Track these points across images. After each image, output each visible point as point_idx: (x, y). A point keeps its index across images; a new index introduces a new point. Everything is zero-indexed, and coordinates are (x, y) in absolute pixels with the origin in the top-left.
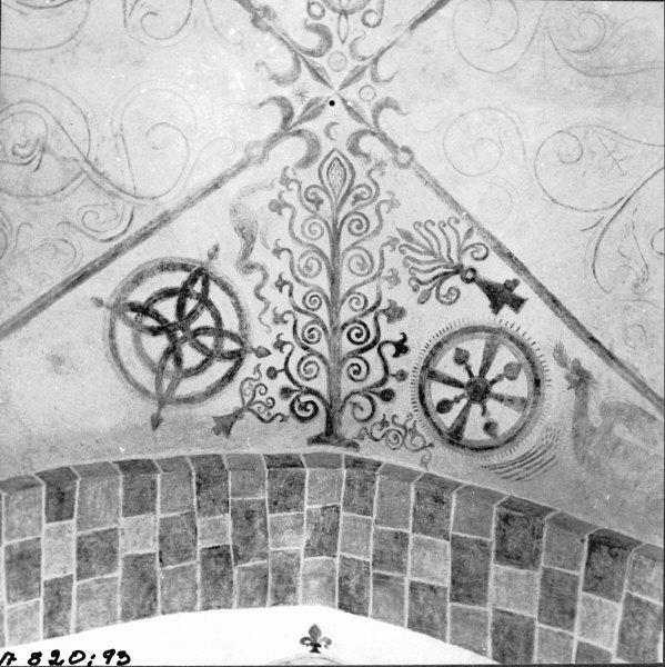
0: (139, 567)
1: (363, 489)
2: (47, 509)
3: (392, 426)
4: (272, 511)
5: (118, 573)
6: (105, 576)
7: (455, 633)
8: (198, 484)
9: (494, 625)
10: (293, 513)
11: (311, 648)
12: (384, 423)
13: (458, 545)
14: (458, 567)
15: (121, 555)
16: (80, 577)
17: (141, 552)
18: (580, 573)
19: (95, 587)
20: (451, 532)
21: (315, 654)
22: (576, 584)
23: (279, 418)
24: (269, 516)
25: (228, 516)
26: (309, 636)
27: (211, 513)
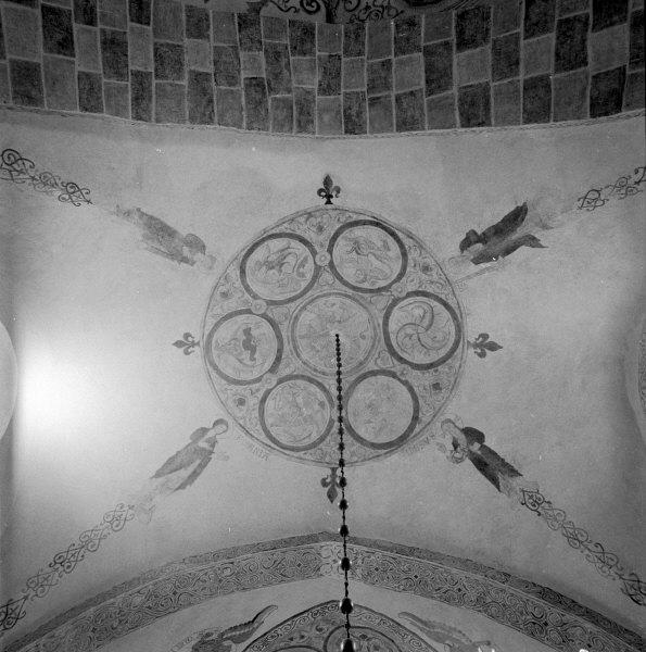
0: (199, 78)
1: (357, 36)
2: (130, 10)
3: (373, 8)
4: (293, 55)
5: (185, 83)
6: (176, 82)
7: (432, 120)
8: (240, 25)
9: (460, 99)
10: (308, 57)
11: (325, 200)
12: (367, 7)
13: (428, 52)
14: (429, 69)
15: (186, 69)
16: (157, 76)
17: (201, 70)
18: (521, 30)
19: (169, 88)
20: (423, 44)
21: (329, 206)
22: (518, 38)
23: (293, 10)
24: (291, 58)
25: (262, 53)
26: (323, 187)
27: (250, 50)
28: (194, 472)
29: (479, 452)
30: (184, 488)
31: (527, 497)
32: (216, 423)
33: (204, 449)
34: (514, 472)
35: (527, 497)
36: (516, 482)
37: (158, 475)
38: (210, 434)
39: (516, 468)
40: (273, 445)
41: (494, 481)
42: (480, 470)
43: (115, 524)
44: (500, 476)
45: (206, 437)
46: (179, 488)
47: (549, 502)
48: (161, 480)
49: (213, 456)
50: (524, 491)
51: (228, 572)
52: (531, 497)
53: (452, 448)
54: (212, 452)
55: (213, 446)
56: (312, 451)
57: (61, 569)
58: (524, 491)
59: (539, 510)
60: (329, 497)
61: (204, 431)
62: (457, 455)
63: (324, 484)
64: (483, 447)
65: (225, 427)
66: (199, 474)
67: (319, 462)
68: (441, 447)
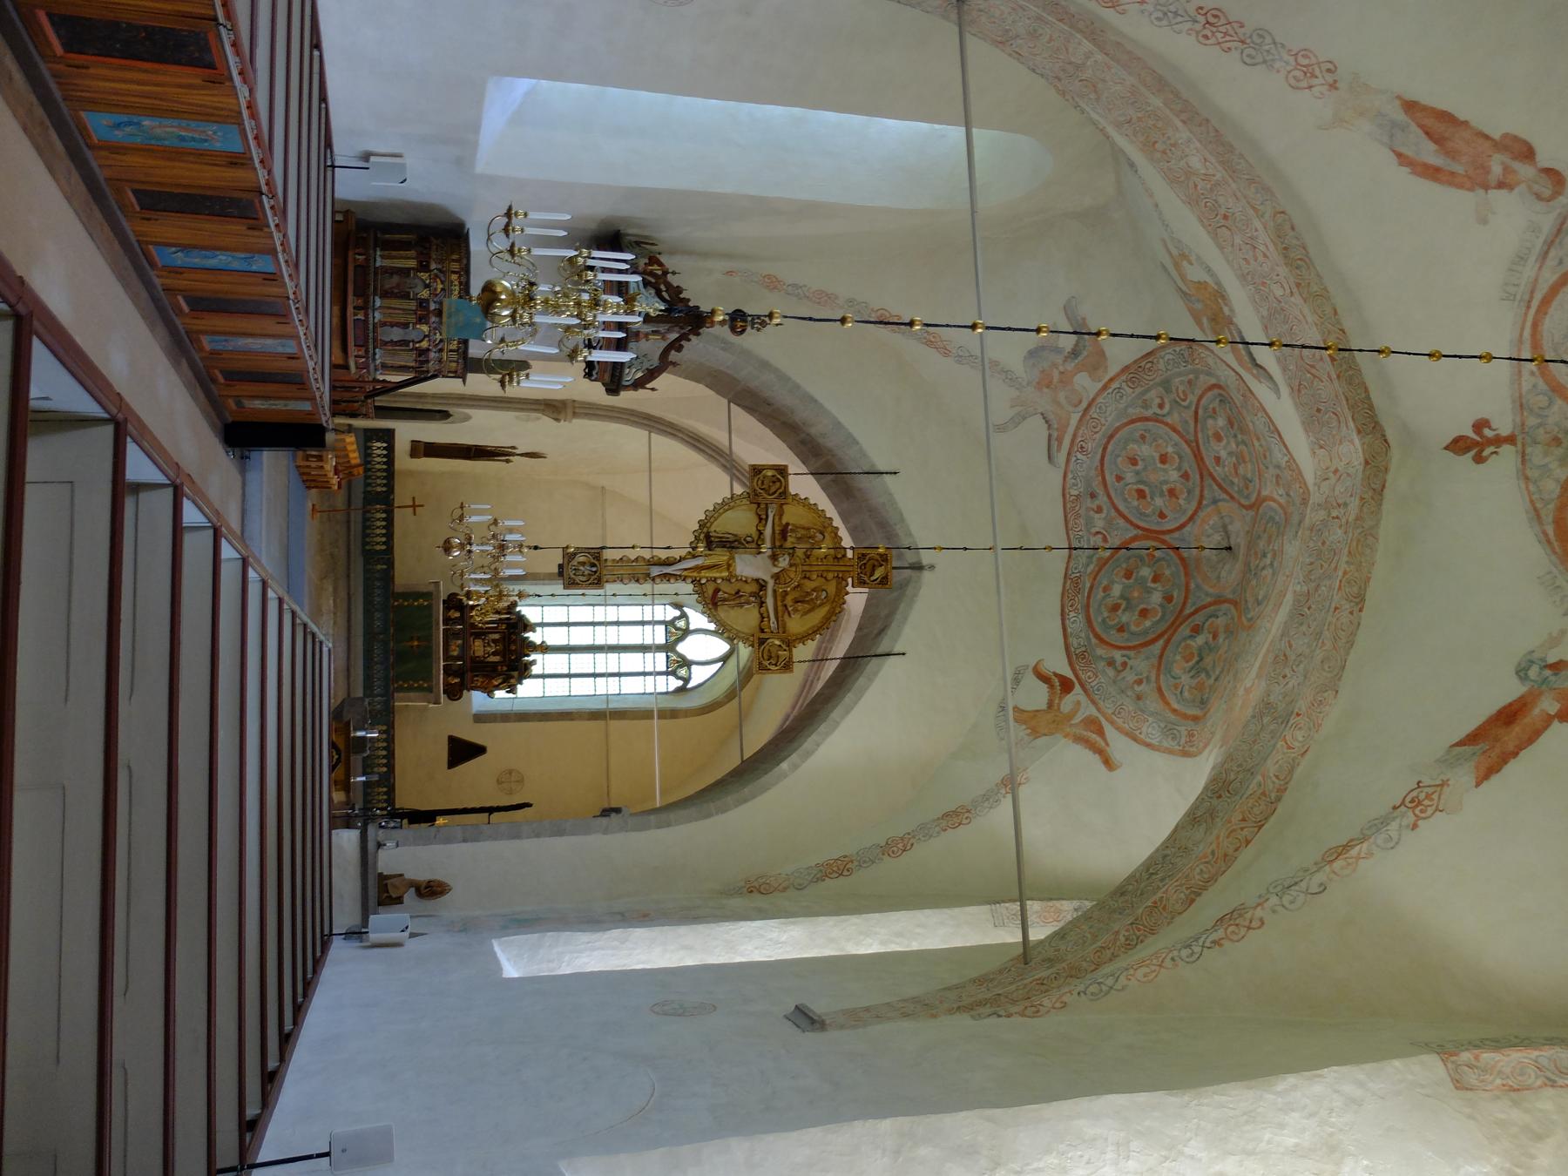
28: (1437, 170)
29: (1536, 711)
30: (1401, 164)
31: (1430, 790)
32: (1549, 171)
33: (1487, 171)
34: (1488, 772)
35: (1430, 790)
36: (1463, 777)
37: (1410, 107)
38: (1525, 171)
39: (1495, 779)
40: (1535, 303)
41: (1472, 738)
42: (1500, 712)
43: (1297, 73)
44: (1483, 746)
45: (1516, 165)
46: (1399, 155)
47: (1415, 826)
48: (1400, 116)
49: (1481, 192)
50: (1442, 785)
51: (1279, 292)
52: (1428, 796)
53: (1551, 660)
54: (1486, 187)
55: (1501, 185)
56: (1542, 385)
57: (1198, 27)
58: (1442, 785)
59: (1403, 809)
60: (1457, 440)
61: (1527, 153)
62: (1533, 672)
63: (1479, 426)
64: (1548, 720)
65: (1547, 193)
66: (1436, 180)
67: (1521, 405)
68: (1554, 641)
